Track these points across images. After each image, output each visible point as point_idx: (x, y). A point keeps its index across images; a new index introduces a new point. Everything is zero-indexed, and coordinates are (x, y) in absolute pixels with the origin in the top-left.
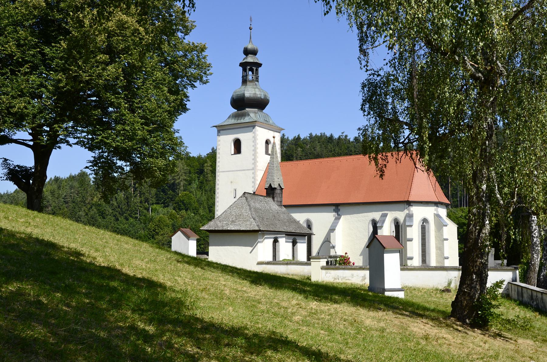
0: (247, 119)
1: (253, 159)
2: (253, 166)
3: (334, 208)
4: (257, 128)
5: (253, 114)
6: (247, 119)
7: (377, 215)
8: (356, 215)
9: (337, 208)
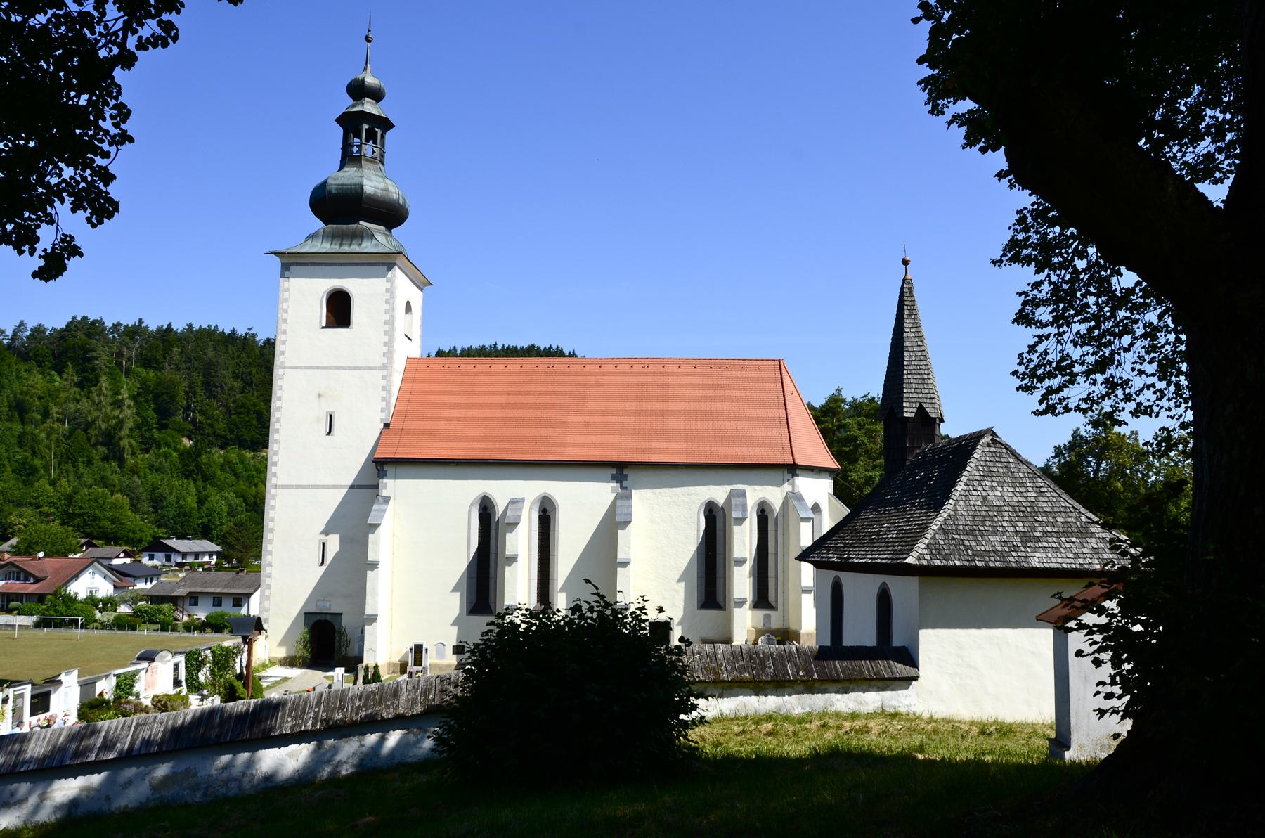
0: (367, 246)
1: (385, 344)
2: (385, 360)
3: (614, 471)
4: (397, 270)
5: (380, 240)
6: (367, 246)
7: (719, 493)
8: (666, 490)
9: (622, 474)
